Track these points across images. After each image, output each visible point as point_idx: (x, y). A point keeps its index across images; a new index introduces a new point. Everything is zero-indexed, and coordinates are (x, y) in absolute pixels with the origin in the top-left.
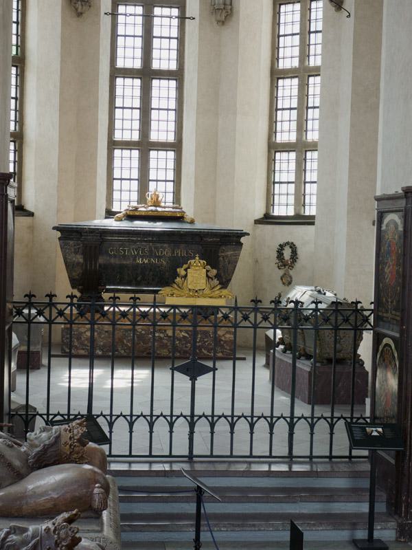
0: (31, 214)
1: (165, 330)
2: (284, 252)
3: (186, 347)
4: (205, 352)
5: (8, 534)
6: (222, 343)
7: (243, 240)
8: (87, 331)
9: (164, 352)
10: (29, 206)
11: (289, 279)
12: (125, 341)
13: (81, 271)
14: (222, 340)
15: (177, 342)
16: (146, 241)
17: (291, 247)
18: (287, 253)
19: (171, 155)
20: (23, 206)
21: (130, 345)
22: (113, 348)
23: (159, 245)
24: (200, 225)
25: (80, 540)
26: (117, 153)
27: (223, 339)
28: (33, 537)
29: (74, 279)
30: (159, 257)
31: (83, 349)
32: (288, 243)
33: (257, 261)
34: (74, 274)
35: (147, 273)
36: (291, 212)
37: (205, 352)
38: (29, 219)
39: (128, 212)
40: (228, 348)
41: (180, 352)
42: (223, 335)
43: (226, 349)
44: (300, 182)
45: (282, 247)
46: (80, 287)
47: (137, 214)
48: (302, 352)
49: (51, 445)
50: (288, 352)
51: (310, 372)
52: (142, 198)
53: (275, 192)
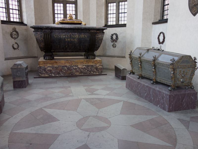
0: (26, 25)
1: (78, 66)
2: (113, 37)
3: (85, 71)
4: (92, 73)
7: (104, 31)
9: (78, 74)
10: (25, 22)
11: (115, 46)
12: (63, 70)
13: (44, 44)
15: (82, 70)
16: (68, 32)
17: (116, 35)
18: (114, 37)
19: (74, 5)
20: (23, 22)
21: (64, 72)
23: (73, 33)
24: (88, 26)
27: (98, 67)
30: (74, 38)
31: (47, 74)
32: (115, 34)
34: (41, 46)
35: (70, 44)
36: (114, 23)
37: (92, 73)
38: (25, 27)
39: (61, 21)
40: (100, 71)
41: (83, 73)
42: (98, 66)
43: (99, 71)
44: (118, 13)
46: (44, 51)
47: (64, 22)
48: (154, 81)
50: (132, 74)
51: (170, 95)
53: (109, 17)
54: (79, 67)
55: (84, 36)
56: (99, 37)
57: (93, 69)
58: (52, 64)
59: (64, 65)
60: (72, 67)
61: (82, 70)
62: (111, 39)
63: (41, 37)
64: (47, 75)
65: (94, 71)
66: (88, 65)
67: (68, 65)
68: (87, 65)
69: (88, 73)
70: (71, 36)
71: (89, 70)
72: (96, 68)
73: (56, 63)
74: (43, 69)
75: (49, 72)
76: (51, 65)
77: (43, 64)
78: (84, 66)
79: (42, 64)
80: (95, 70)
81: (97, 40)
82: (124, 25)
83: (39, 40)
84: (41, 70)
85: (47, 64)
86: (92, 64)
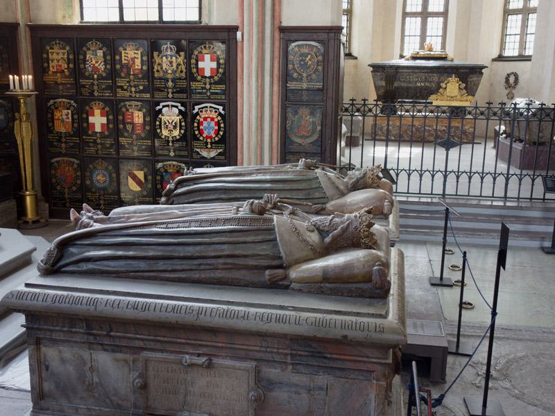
0: (356, 58)
5: (334, 217)
7: (483, 71)
9: (432, 139)
10: (355, 53)
18: (512, 79)
22: (400, 136)
23: (431, 75)
24: (457, 62)
25: (374, 224)
26: (408, 19)
28: (347, 220)
32: (513, 73)
33: (492, 85)
36: (516, 54)
38: (355, 60)
45: (508, 75)
48: (518, 138)
49: (361, 178)
51: (521, 150)
52: (422, 47)
62: (506, 82)
82: (528, 59)
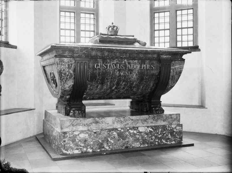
1: (137, 128)
3: (152, 139)
4: (164, 141)
6: (174, 133)
7: (184, 57)
8: (80, 133)
12: (109, 139)
14: (174, 132)
21: (112, 141)
22: (101, 146)
23: (131, 61)
27: (175, 130)
29: (65, 91)
37: (164, 141)
41: (148, 144)
42: (175, 128)
43: (177, 138)
54: (141, 129)
55: (150, 66)
56: (175, 69)
57: (165, 133)
58: (88, 125)
59: (112, 127)
60: (128, 130)
61: (146, 136)
63: (69, 68)
64: (76, 152)
65: (168, 137)
66: (157, 125)
67: (118, 126)
68: (153, 125)
69: (157, 143)
70: (125, 66)
71: (159, 136)
72: (172, 132)
73: (97, 122)
74: (70, 137)
75: (82, 145)
76: (85, 128)
77: (69, 126)
78: (149, 129)
79: (67, 127)
80: (169, 135)
81: (171, 74)
83: (65, 74)
84: (66, 139)
85: (78, 127)
86: (163, 123)
